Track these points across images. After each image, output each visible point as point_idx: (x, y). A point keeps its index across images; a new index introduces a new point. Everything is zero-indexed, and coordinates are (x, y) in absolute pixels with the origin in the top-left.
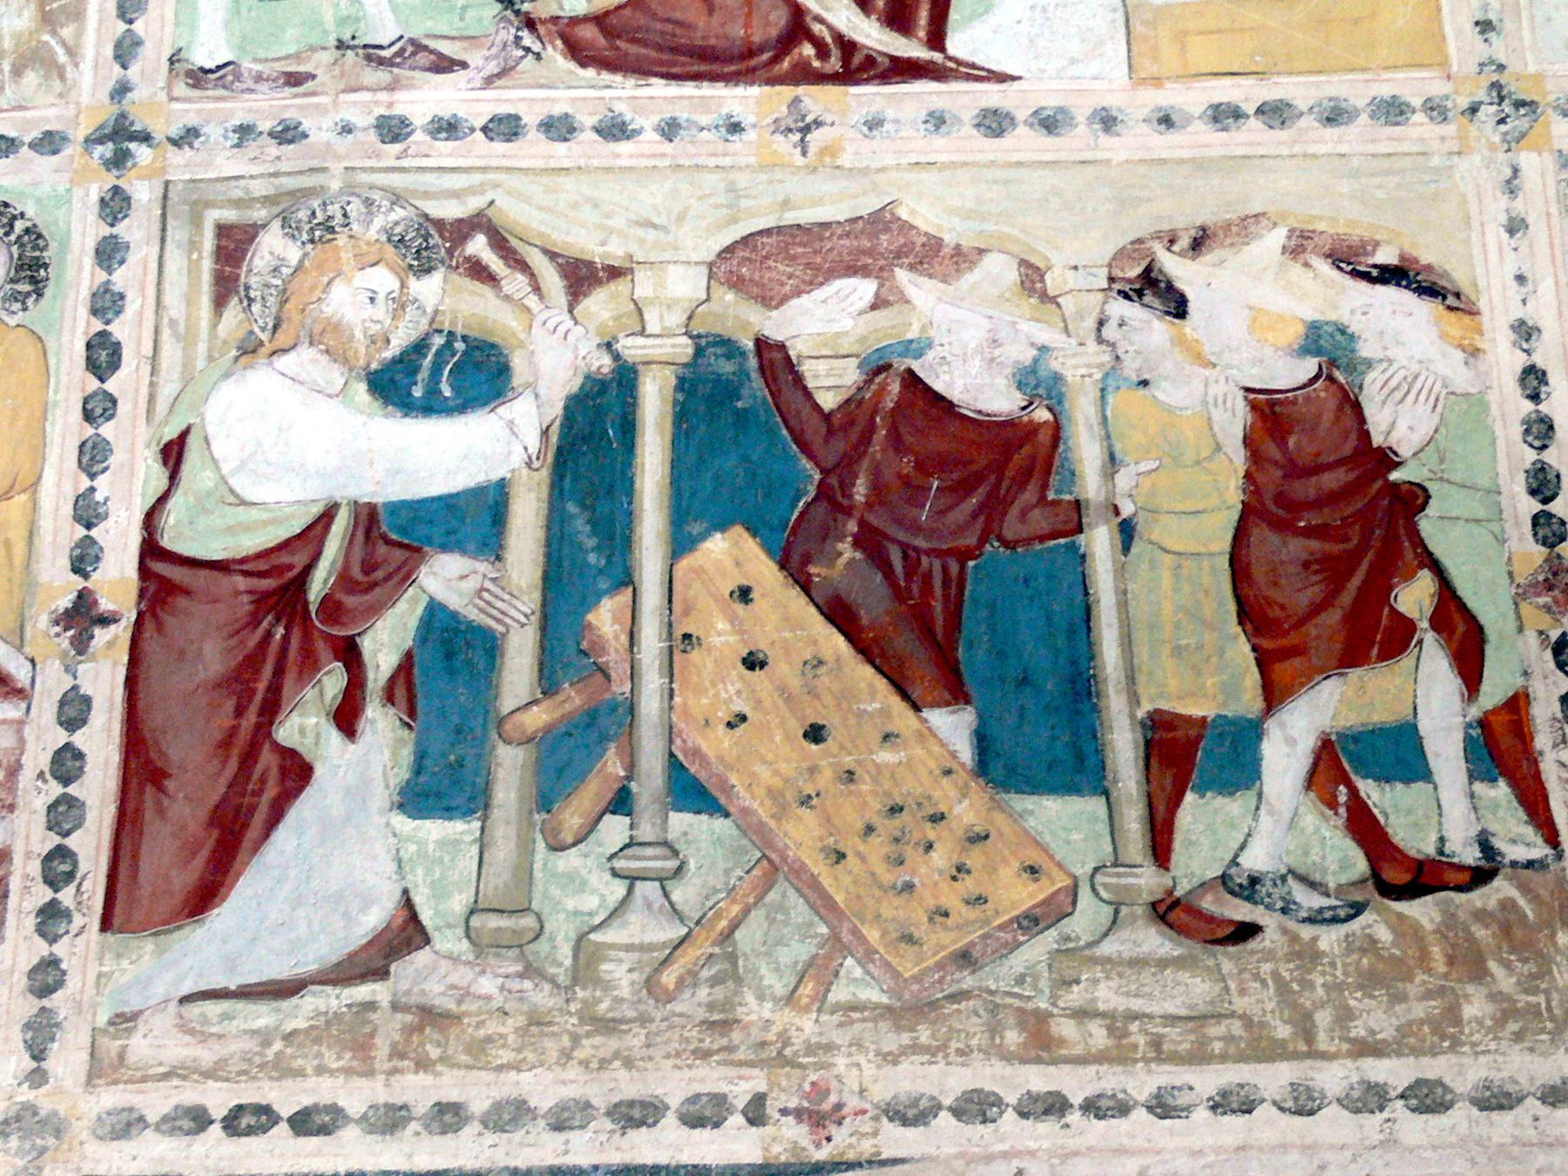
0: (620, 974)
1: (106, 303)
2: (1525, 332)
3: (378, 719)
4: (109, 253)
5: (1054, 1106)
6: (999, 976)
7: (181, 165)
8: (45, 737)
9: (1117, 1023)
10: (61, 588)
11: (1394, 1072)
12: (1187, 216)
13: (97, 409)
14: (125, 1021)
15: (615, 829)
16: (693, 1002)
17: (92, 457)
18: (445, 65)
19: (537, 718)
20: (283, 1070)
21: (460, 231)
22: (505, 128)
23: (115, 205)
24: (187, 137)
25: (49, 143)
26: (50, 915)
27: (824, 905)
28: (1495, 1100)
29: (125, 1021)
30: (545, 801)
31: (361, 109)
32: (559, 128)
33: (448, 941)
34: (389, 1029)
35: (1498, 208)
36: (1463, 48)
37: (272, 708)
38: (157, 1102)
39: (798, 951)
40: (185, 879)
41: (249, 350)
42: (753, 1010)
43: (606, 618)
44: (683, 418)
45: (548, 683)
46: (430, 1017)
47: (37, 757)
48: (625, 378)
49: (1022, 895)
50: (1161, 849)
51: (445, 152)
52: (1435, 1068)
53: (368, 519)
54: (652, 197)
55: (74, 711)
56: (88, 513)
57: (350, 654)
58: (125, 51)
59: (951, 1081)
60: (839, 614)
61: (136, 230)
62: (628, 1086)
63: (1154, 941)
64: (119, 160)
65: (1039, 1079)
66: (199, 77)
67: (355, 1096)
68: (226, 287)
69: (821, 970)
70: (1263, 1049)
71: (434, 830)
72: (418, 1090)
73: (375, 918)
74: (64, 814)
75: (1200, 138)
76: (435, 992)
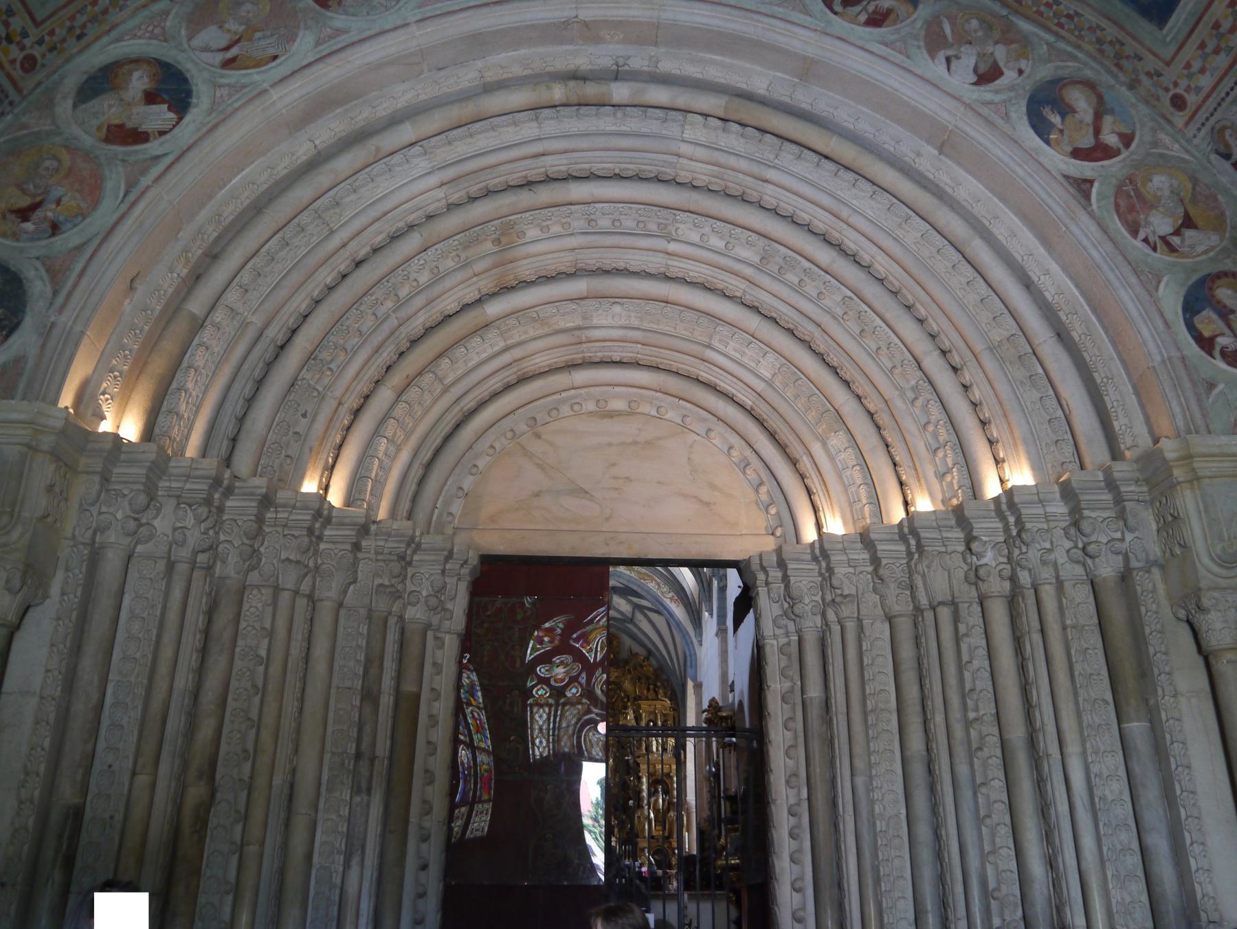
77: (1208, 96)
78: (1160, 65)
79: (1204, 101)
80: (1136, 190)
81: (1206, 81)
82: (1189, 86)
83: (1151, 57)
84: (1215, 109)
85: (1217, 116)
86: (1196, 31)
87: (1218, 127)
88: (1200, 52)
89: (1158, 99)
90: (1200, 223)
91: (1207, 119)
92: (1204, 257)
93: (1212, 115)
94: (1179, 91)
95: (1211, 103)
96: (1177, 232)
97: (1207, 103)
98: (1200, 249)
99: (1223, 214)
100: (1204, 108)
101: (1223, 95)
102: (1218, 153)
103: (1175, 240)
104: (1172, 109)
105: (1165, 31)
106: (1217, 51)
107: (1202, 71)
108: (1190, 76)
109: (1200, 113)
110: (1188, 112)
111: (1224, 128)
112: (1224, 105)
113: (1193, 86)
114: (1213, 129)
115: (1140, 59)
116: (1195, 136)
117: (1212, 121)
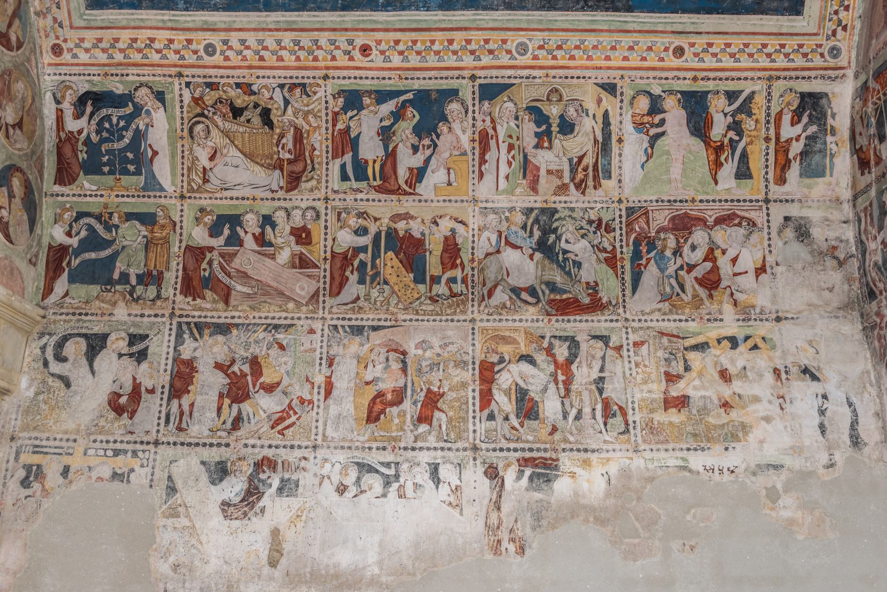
0: (378, 303)
1: (326, 221)
2: (473, 229)
3: (355, 273)
4: (326, 214)
5: (417, 320)
6: (414, 305)
7: (333, 203)
8: (322, 274)
9: (425, 311)
10: (323, 255)
11: (450, 318)
12: (440, 214)
13: (326, 234)
14: (332, 307)
15: (378, 287)
16: (385, 307)
17: (326, 240)
18: (361, 192)
19: (371, 273)
20: (347, 313)
21: (363, 213)
22: (368, 200)
23: (326, 208)
24: (334, 200)
25: (319, 199)
26: (324, 295)
27: (398, 296)
28: (458, 321)
29: (332, 307)
30: (371, 283)
31: (352, 197)
32: (374, 200)
33: (362, 299)
34: (357, 309)
35: (472, 214)
36: (471, 193)
37: (345, 271)
38: (335, 316)
39: (395, 302)
40: (337, 291)
41: (341, 227)
42: (391, 308)
43: (378, 261)
44: (386, 237)
45: (372, 269)
46: (360, 308)
47: (322, 276)
48: (380, 232)
49: (416, 296)
50: (430, 291)
51: (362, 203)
52: (453, 317)
53: (354, 248)
54: (383, 210)
55: (325, 270)
56: (325, 246)
57: (352, 265)
58: (327, 187)
59: (408, 317)
60: (401, 262)
61: (329, 212)
62: (379, 317)
63: (428, 302)
64: (327, 202)
65: (417, 317)
66: (335, 192)
67: (354, 317)
68: (339, 220)
69: (397, 304)
70: (438, 315)
71: (361, 286)
72: (359, 316)
73: (355, 296)
74: (325, 283)
75: (441, 204)
76: (361, 305)
77: (77, 65)
78: (66, 23)
79: (72, 65)
80: (9, 82)
81: (84, 57)
82: (72, 50)
83: (66, 15)
84: (75, 75)
85: (73, 78)
86: (104, 31)
87: (68, 83)
88: (95, 42)
89: (47, 36)
90: (24, 129)
91: (66, 74)
92: (17, 152)
93: (70, 75)
94: (63, 45)
95: (75, 70)
96: (13, 126)
97: (74, 68)
98: (18, 146)
99: (35, 131)
100: (68, 68)
101: (86, 72)
102: (54, 94)
103: (11, 131)
104: (49, 49)
105: (87, 12)
106: (104, 50)
107: (87, 50)
108: (77, 46)
109: (64, 67)
110: (57, 60)
111: (71, 88)
112: (82, 77)
113: (74, 52)
114: (64, 81)
115: (59, 7)
116: (49, 75)
117: (67, 78)
